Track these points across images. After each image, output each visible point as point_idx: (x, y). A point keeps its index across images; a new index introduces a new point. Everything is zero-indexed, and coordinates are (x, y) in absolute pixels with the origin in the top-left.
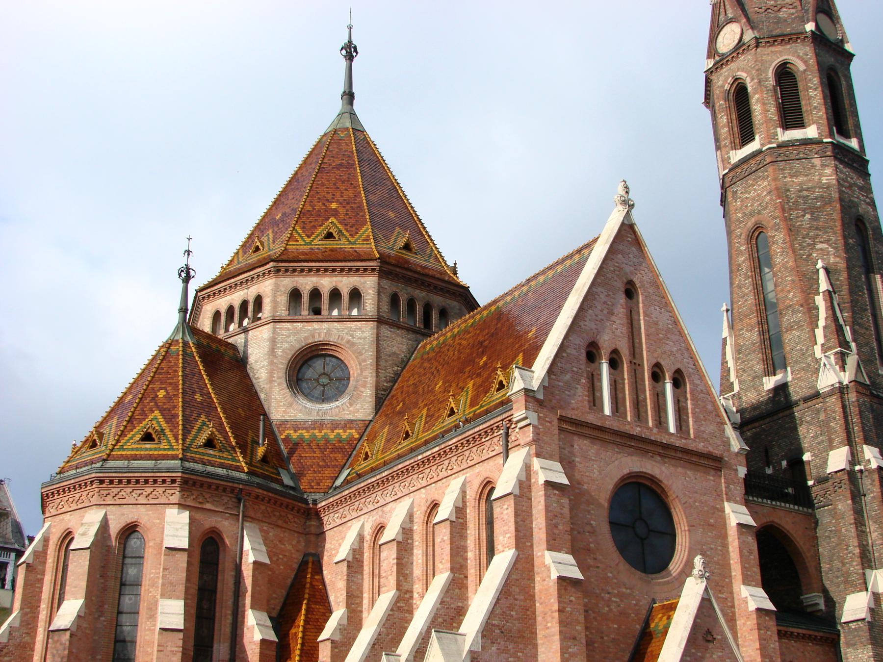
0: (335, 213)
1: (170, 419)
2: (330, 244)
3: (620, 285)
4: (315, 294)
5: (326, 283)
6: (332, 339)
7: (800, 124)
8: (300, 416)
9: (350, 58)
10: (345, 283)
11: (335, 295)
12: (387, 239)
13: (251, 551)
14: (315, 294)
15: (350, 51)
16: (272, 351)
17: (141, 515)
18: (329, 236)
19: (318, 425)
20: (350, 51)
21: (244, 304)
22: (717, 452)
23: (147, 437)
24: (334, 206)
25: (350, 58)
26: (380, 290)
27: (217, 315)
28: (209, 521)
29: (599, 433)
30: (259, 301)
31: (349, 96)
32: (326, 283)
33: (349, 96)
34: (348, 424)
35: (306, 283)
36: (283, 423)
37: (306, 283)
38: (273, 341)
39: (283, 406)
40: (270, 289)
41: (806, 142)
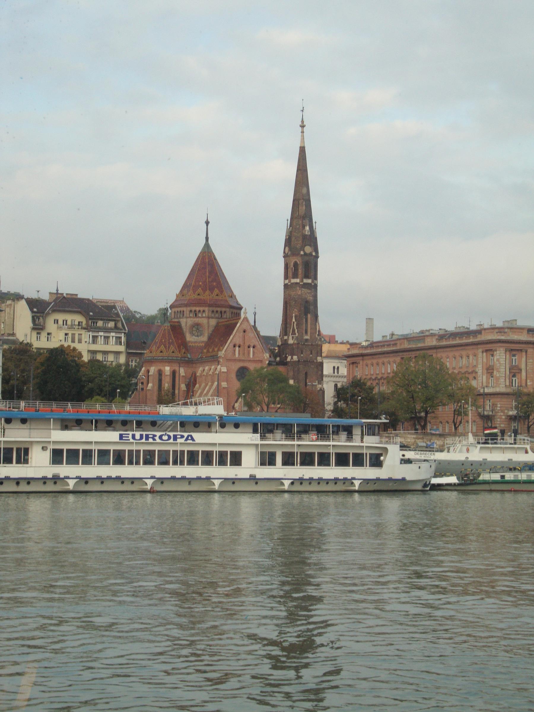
0: (200, 286)
1: (165, 347)
2: (199, 297)
3: (242, 331)
4: (195, 311)
5: (197, 309)
6: (199, 322)
7: (297, 278)
8: (193, 340)
9: (207, 225)
10: (202, 309)
11: (199, 311)
12: (212, 293)
13: (182, 371)
14: (195, 311)
15: (207, 223)
16: (186, 325)
17: (162, 368)
18: (199, 295)
19: (195, 342)
20: (207, 223)
21: (180, 312)
22: (261, 359)
23: (161, 352)
24: (201, 283)
25: (207, 225)
26: (209, 311)
27: (175, 312)
28: (174, 368)
29: (235, 360)
30: (183, 312)
31: (207, 239)
32: (197, 309)
33: (207, 239)
34: (203, 342)
35: (194, 309)
36: (189, 342)
37: (194, 309)
38: (186, 322)
39: (189, 338)
40: (186, 310)
41: (297, 283)
